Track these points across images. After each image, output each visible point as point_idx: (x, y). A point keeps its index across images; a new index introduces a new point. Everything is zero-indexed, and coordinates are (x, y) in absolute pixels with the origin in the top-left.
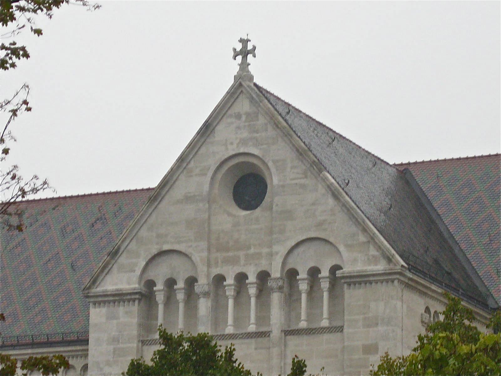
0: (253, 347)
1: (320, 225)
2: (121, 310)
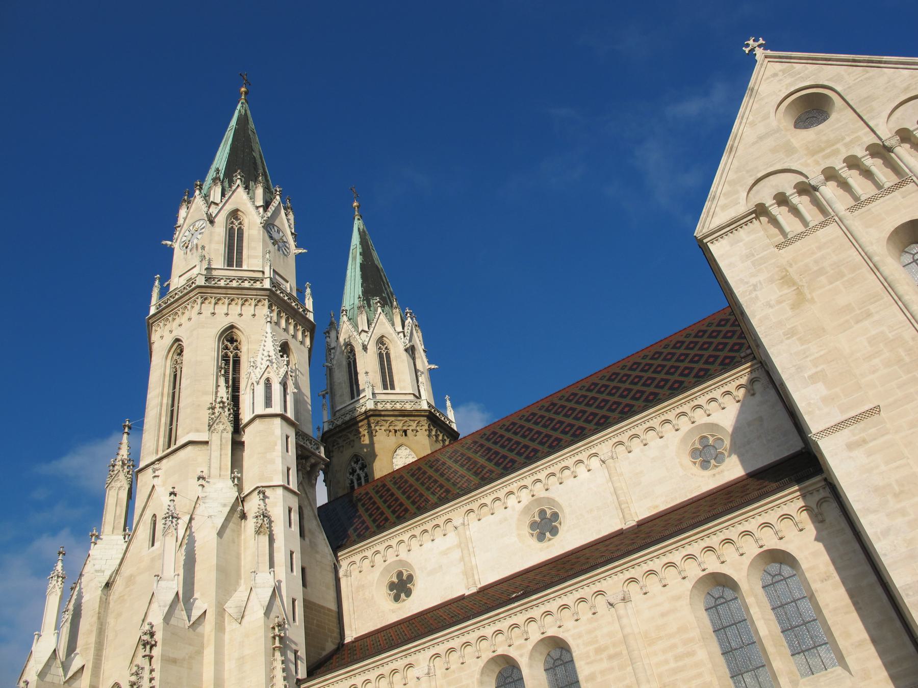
1: (907, 89)
2: (742, 233)
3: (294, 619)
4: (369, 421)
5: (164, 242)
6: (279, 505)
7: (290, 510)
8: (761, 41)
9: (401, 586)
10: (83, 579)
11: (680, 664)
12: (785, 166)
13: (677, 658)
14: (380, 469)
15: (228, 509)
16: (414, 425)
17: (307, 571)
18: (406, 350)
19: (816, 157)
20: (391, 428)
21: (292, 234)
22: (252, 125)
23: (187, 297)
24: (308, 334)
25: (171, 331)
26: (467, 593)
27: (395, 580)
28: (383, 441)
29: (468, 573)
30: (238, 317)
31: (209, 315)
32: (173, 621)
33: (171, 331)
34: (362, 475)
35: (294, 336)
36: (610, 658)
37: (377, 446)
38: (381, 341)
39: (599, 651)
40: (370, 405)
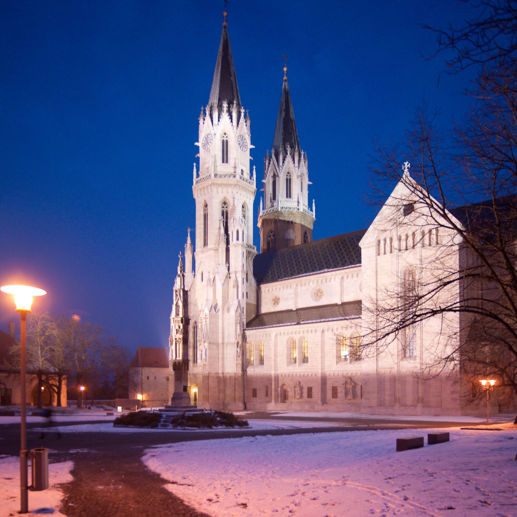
6: (240, 277)
9: (276, 301)
15: (225, 277)
29: (296, 302)
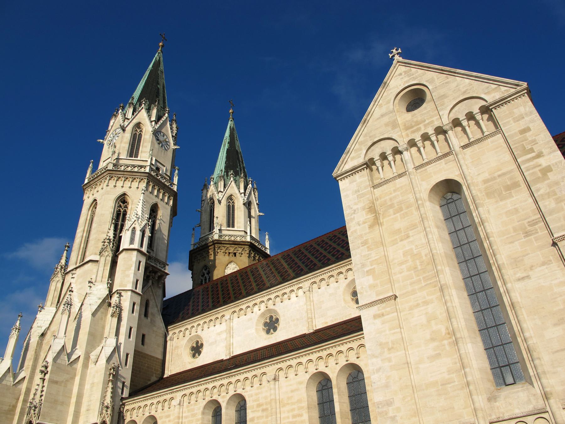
0: (444, 163)
1: (465, 92)
2: (357, 177)
3: (126, 364)
4: (215, 246)
5: (99, 140)
6: (126, 301)
7: (134, 304)
8: (400, 51)
9: (197, 350)
10: (33, 330)
11: (294, 420)
12: (389, 136)
13: (294, 416)
14: (217, 274)
15: (101, 300)
16: (240, 250)
17: (146, 337)
18: (244, 204)
19: (408, 131)
20: (227, 251)
21: (173, 136)
22: (162, 67)
23: (102, 176)
24: (172, 198)
25: (93, 195)
26: (225, 358)
27: (195, 345)
28: (221, 258)
29: (229, 347)
30: (128, 188)
31: (113, 187)
32: (59, 361)
33: (93, 195)
34: (208, 278)
35: (162, 200)
36: (263, 410)
37: (217, 261)
38: (230, 198)
39: (259, 405)
40: (216, 237)
